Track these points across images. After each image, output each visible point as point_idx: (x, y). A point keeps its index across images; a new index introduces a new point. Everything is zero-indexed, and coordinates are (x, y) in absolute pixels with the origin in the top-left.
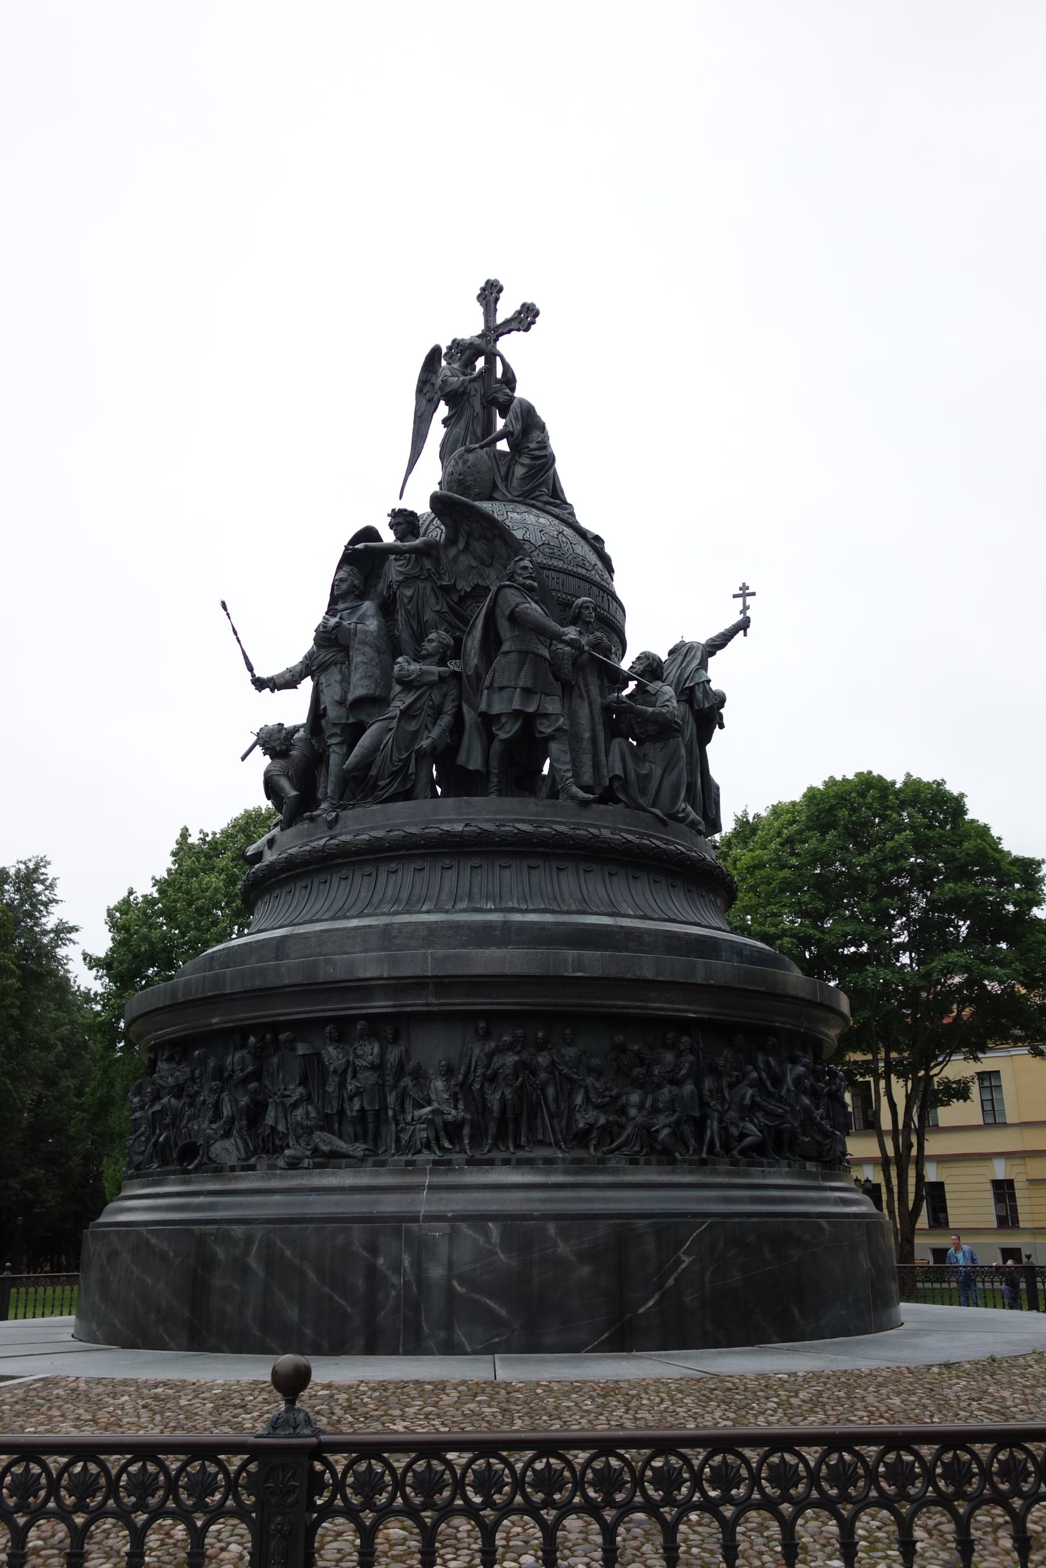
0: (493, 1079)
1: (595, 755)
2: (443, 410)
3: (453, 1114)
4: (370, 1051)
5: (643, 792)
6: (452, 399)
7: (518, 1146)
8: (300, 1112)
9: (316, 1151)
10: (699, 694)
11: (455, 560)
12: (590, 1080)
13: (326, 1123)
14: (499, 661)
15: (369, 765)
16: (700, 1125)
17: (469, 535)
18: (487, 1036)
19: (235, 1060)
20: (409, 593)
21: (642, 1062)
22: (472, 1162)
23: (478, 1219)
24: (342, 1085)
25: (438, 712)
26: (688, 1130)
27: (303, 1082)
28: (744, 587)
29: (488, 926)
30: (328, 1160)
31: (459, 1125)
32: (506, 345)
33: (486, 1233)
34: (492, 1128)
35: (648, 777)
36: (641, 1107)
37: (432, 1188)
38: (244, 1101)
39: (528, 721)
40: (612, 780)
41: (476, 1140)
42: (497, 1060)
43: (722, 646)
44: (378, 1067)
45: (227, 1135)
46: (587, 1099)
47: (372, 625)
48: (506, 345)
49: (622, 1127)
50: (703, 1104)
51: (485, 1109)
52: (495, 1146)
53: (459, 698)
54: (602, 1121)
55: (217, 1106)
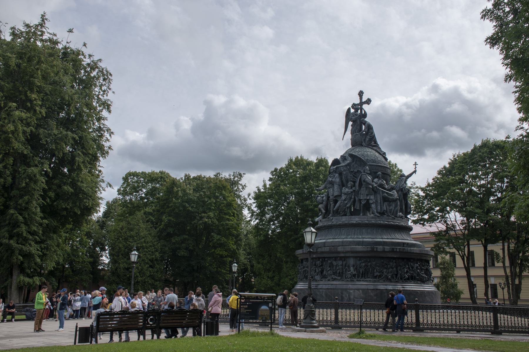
0: (361, 267)
1: (381, 205)
2: (351, 123)
3: (354, 273)
4: (340, 263)
5: (390, 212)
6: (353, 121)
7: (365, 278)
8: (329, 272)
9: (332, 278)
10: (403, 190)
11: (353, 166)
12: (377, 268)
13: (334, 274)
14: (362, 189)
15: (338, 209)
16: (396, 275)
17: (356, 160)
18: (360, 260)
19: (318, 262)
20: (345, 173)
21: (386, 264)
22: (357, 281)
23: (358, 290)
24: (336, 268)
25: (351, 198)
26: (394, 276)
27: (330, 267)
28: (416, 163)
29: (360, 242)
30: (334, 280)
31: (355, 275)
32: (365, 107)
33: (359, 291)
34: (361, 276)
35: (391, 209)
36: (386, 272)
37: (351, 284)
38: (320, 270)
39: (368, 200)
40: (384, 211)
41: (358, 277)
42: (361, 264)
43: (410, 177)
44: (342, 265)
45: (317, 275)
46: (377, 271)
47: (338, 180)
48: (365, 107)
49: (382, 275)
50: (397, 272)
51: (360, 272)
52: (361, 278)
53: (355, 195)
54: (379, 274)
55: (315, 270)
